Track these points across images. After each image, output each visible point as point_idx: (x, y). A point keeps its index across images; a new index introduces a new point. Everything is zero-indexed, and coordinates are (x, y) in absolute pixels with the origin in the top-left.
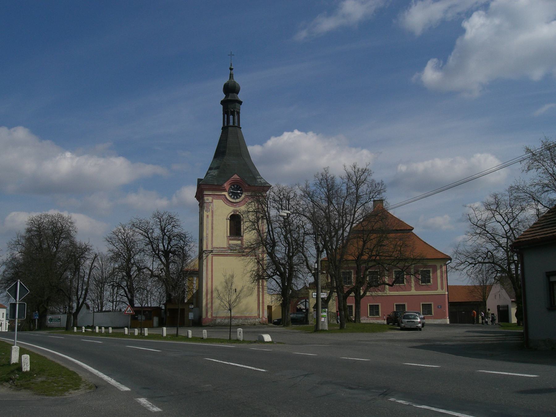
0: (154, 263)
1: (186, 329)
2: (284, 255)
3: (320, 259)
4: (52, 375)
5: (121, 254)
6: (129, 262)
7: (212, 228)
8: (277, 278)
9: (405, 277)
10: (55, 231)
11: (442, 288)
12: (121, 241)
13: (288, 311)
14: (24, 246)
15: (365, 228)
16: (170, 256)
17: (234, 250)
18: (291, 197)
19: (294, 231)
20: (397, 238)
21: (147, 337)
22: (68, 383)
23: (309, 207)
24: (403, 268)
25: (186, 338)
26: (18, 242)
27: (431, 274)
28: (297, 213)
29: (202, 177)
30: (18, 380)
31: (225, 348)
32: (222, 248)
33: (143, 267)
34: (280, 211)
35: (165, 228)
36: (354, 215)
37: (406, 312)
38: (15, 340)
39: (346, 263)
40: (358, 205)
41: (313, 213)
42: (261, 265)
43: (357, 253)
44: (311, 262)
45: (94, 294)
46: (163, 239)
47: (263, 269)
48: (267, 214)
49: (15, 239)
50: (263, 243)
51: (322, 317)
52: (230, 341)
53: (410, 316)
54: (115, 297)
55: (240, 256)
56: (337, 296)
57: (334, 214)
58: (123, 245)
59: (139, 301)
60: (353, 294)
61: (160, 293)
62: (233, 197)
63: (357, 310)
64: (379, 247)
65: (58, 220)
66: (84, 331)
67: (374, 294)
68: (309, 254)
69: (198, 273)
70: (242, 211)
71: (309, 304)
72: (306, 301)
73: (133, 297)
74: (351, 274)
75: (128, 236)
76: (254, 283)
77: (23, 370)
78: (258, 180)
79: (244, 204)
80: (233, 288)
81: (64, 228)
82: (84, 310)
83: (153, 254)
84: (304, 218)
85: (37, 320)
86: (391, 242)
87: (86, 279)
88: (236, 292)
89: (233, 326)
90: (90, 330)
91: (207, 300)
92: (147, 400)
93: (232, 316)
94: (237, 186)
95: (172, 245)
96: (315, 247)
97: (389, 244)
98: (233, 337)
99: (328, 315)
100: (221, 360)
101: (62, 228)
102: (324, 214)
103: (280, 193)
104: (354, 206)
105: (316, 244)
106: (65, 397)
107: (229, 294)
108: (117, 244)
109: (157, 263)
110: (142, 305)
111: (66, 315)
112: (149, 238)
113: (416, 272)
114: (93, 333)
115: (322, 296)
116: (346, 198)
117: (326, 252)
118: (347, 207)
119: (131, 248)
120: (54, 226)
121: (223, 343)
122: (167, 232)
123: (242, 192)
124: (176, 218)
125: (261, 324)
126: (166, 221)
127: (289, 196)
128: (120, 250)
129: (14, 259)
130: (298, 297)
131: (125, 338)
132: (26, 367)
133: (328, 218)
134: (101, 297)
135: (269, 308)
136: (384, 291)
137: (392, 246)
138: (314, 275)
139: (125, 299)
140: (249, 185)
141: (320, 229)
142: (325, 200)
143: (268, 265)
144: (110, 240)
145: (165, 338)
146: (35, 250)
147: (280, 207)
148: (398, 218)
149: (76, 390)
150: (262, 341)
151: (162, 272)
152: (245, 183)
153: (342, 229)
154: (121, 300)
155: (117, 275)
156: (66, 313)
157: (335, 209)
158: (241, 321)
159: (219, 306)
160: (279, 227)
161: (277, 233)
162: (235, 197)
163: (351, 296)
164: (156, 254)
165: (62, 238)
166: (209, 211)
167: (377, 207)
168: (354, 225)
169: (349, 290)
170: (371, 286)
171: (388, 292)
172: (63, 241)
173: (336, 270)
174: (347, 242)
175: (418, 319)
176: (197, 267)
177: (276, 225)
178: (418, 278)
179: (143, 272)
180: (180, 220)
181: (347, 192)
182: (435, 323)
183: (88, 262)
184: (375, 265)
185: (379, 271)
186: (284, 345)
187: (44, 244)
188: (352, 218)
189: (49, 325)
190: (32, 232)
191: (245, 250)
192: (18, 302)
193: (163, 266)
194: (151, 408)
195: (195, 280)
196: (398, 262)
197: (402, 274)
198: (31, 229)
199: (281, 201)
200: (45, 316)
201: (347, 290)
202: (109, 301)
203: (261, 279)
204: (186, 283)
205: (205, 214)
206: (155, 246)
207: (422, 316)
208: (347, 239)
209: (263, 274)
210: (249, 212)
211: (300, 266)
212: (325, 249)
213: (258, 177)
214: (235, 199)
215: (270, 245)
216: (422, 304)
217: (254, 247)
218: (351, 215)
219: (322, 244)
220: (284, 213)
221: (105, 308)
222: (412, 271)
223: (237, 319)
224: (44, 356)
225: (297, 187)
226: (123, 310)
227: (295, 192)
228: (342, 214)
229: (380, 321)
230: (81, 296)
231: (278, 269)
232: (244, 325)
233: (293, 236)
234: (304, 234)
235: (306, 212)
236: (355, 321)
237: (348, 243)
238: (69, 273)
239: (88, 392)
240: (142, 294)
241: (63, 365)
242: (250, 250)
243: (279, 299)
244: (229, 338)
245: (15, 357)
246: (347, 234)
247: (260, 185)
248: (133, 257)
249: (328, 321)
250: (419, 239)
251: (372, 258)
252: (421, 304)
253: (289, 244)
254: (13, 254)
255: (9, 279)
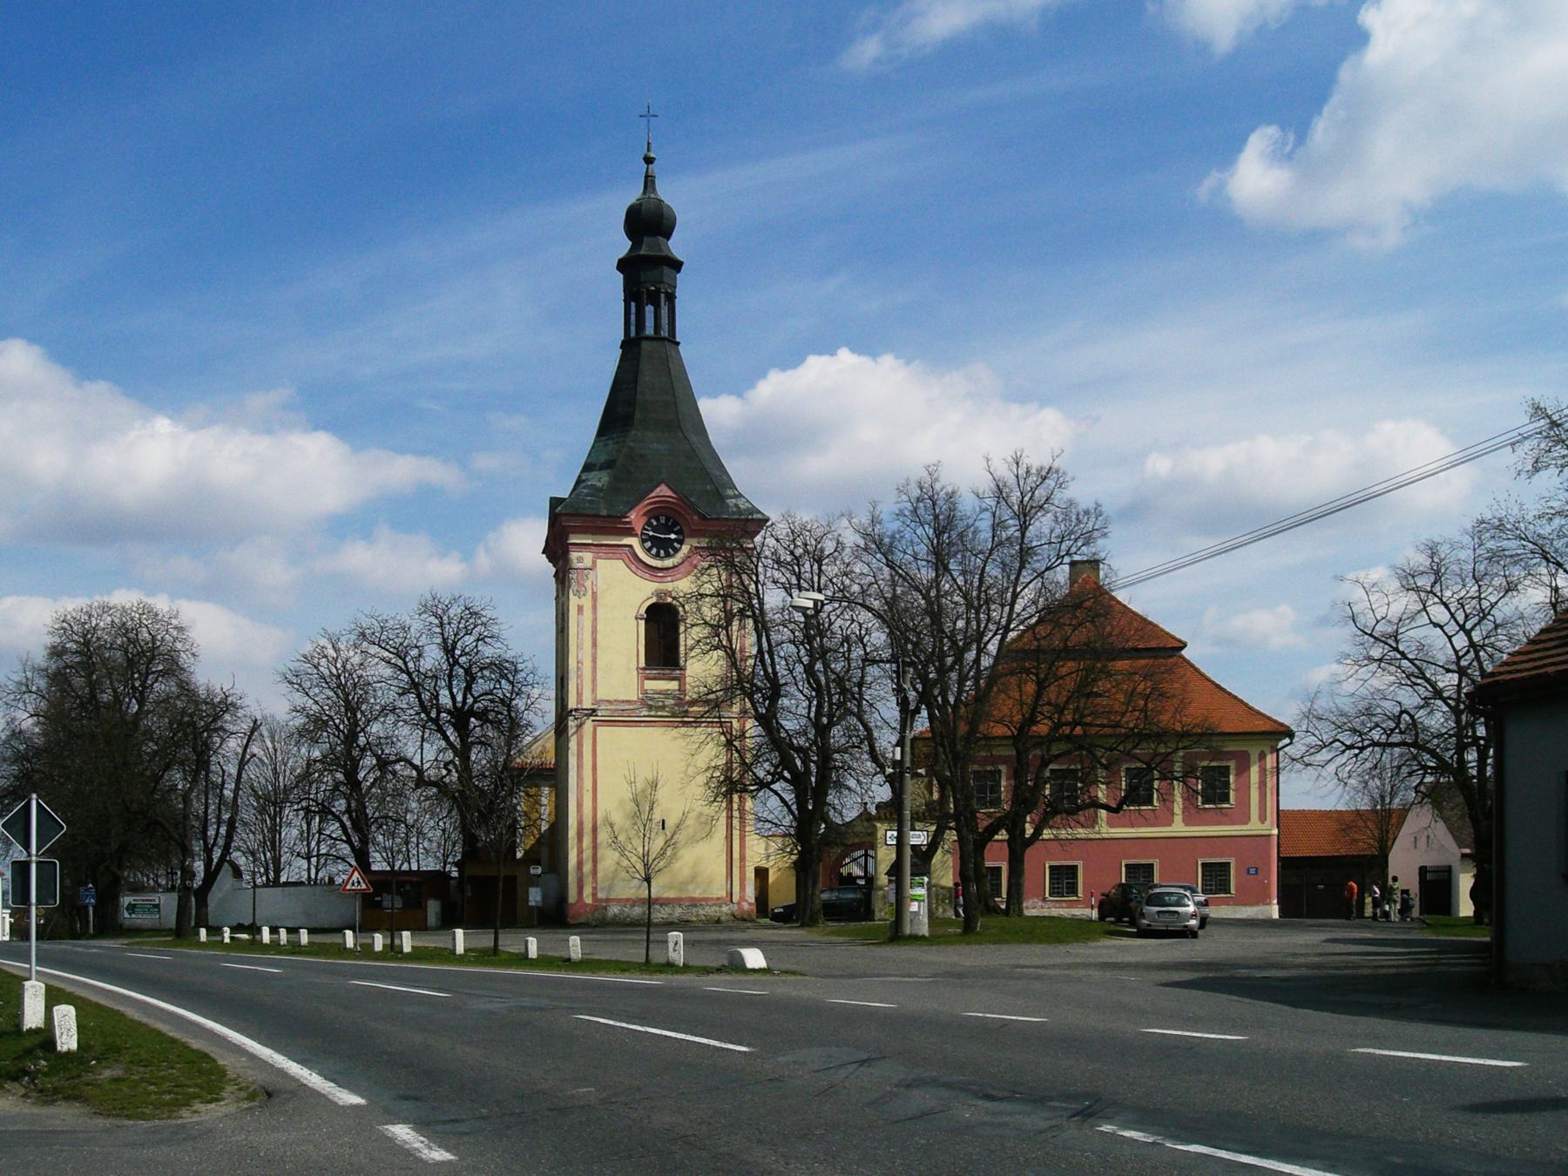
0: (426, 745)
1: (522, 935)
2: (804, 721)
3: (909, 735)
4: (141, 1061)
5: (327, 721)
6: (351, 745)
7: (594, 644)
8: (784, 789)
9: (1156, 784)
10: (132, 653)
11: (1263, 818)
12: (327, 683)
13: (815, 883)
14: (44, 697)
15: (1042, 642)
16: (472, 725)
17: (659, 707)
18: (827, 553)
19: (836, 651)
20: (1136, 673)
21: (409, 957)
22: (188, 1083)
23: (880, 582)
24: (1152, 760)
25: (523, 959)
26: (27, 686)
27: (1232, 778)
28: (846, 599)
29: (564, 493)
30: (45, 1075)
31: (632, 987)
32: (623, 701)
33: (393, 758)
34: (795, 592)
35: (455, 643)
36: (1012, 605)
37: (1156, 886)
38: (30, 964)
39: (985, 745)
40: (1026, 576)
41: (891, 599)
42: (737, 751)
43: (1018, 718)
44: (884, 744)
45: (254, 834)
46: (450, 676)
47: (743, 763)
48: (755, 601)
49: (16, 678)
50: (742, 688)
51: (912, 900)
52: (647, 966)
53: (1167, 898)
54: (313, 844)
55: (676, 724)
56: (955, 841)
57: (952, 603)
58: (335, 693)
59: (384, 854)
60: (1002, 835)
61: (444, 830)
62: (654, 551)
63: (1013, 881)
64: (1083, 701)
65: (140, 619)
66: (227, 940)
67: (1063, 834)
68: (876, 720)
69: (554, 776)
70: (682, 594)
71: (876, 864)
72: (866, 855)
73: (368, 843)
74: (1000, 777)
75: (349, 667)
76: (716, 804)
77: (59, 1048)
78: (728, 501)
79: (689, 573)
80: (657, 816)
81: (158, 643)
82: (225, 881)
83: (422, 719)
84: (864, 616)
85: (91, 909)
86: (1118, 685)
87: (228, 793)
88: (663, 828)
89: (657, 925)
90: (245, 936)
91: (580, 852)
92: (413, 1129)
93: (653, 896)
94: (668, 519)
95: (476, 694)
96: (894, 698)
97: (1114, 690)
98: (657, 957)
99: (929, 895)
100: (621, 1021)
101: (154, 643)
102: (923, 602)
103: (794, 540)
104: (1013, 577)
105: (899, 691)
106: (179, 1122)
107: (645, 835)
108: (317, 690)
109: (435, 747)
110: (394, 865)
111: (175, 896)
112: (409, 674)
113: (1191, 772)
114: (255, 944)
115: (914, 841)
116: (990, 554)
117: (929, 714)
118: (991, 582)
119: (357, 703)
120: (129, 639)
121: (627, 974)
122: (460, 656)
123: (681, 537)
124: (488, 613)
125: (738, 920)
126: (459, 623)
127: (822, 550)
128: (326, 708)
129: (17, 734)
130: (843, 844)
131: (346, 959)
132: (68, 1041)
133: (935, 612)
134: (273, 843)
135: (761, 873)
136: (1094, 827)
137: (1121, 697)
138: (890, 780)
139: (345, 849)
140: (703, 518)
141: (910, 646)
142: (928, 562)
143: (758, 751)
144: (294, 680)
145: (461, 959)
146: (76, 709)
147: (796, 582)
148: (1140, 613)
149: (210, 1102)
150: (738, 966)
151: (449, 771)
152: (689, 511)
153: (974, 646)
154: (333, 852)
155: (319, 781)
156: (173, 888)
157: (956, 587)
158: (680, 910)
159: (616, 870)
160: (790, 642)
161: (786, 660)
162: (662, 552)
163: (998, 841)
164: (430, 719)
165: (154, 673)
166: (584, 595)
167: (1080, 581)
168: (1012, 635)
169: (992, 824)
170: (1055, 812)
171: (1106, 828)
172: (156, 681)
173: (955, 766)
174: (989, 686)
175: (1188, 906)
176: (550, 758)
177: (781, 635)
178: (1195, 788)
179: (394, 773)
180: (499, 621)
181: (993, 537)
182: (1238, 916)
183: (234, 744)
184: (1069, 752)
185: (1082, 769)
186: (803, 978)
187: (103, 692)
188: (1005, 615)
189: (127, 923)
190: (64, 657)
191: (691, 709)
192: (34, 858)
193: (452, 755)
194: (426, 1151)
195: (546, 795)
196: (1138, 745)
197: (1148, 778)
198: (63, 647)
199: (798, 565)
200: (115, 898)
201: (986, 823)
202: (298, 855)
203: (737, 792)
204: (519, 804)
205: (574, 601)
206: (426, 696)
207: (1201, 898)
208: (989, 677)
209: (742, 776)
210: (702, 596)
211: (851, 754)
212: (923, 706)
213: (730, 492)
214: (662, 558)
215: (763, 695)
216: (1204, 865)
217: (718, 698)
218: (1003, 606)
219: (915, 689)
220: (806, 600)
221: (286, 876)
222: (1178, 767)
223: (666, 905)
224: (117, 1008)
225: (845, 523)
226: (338, 880)
227: (841, 539)
228: (977, 603)
229: (1079, 912)
230: (215, 839)
231: (786, 762)
232: (688, 921)
233: (833, 666)
234: (863, 660)
235: (870, 595)
236: (1006, 912)
237: (992, 688)
238: (178, 776)
239: (247, 1109)
240: (393, 835)
241: (171, 1034)
242: (707, 709)
243: (788, 850)
244: (644, 960)
245: (34, 1013)
246: (991, 661)
247: (736, 517)
248: (363, 730)
249: (929, 910)
250: (1202, 675)
251: (1061, 731)
252: (1200, 863)
253: (818, 689)
254: (13, 719)
255: (5, 793)
